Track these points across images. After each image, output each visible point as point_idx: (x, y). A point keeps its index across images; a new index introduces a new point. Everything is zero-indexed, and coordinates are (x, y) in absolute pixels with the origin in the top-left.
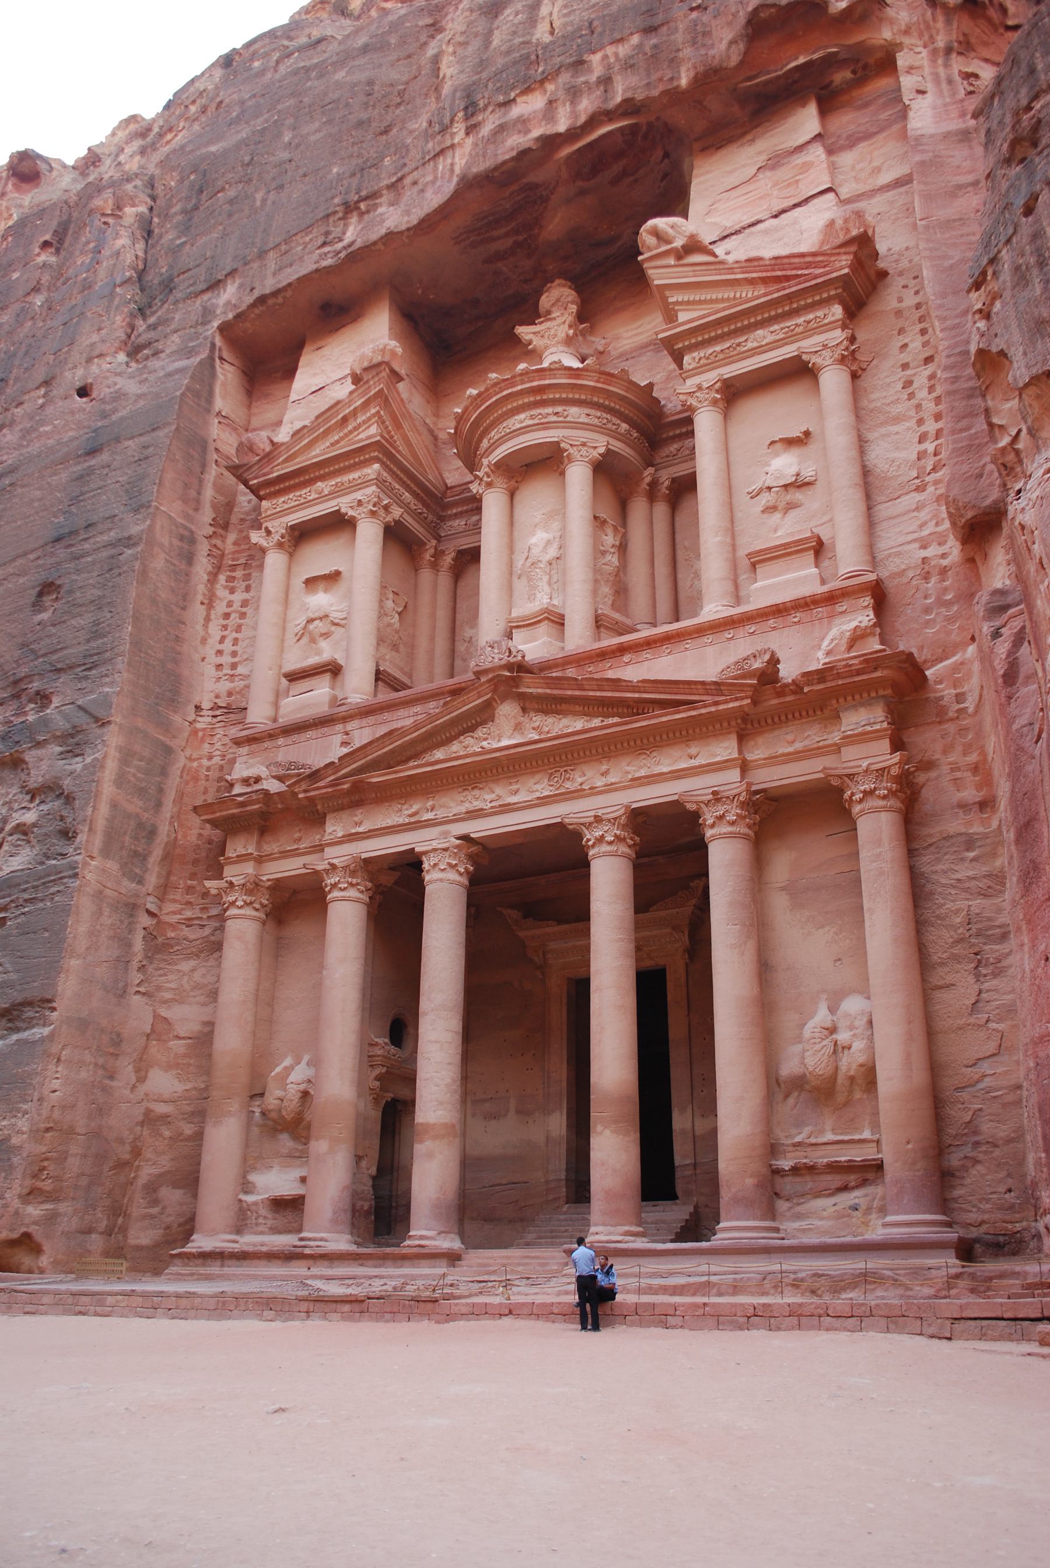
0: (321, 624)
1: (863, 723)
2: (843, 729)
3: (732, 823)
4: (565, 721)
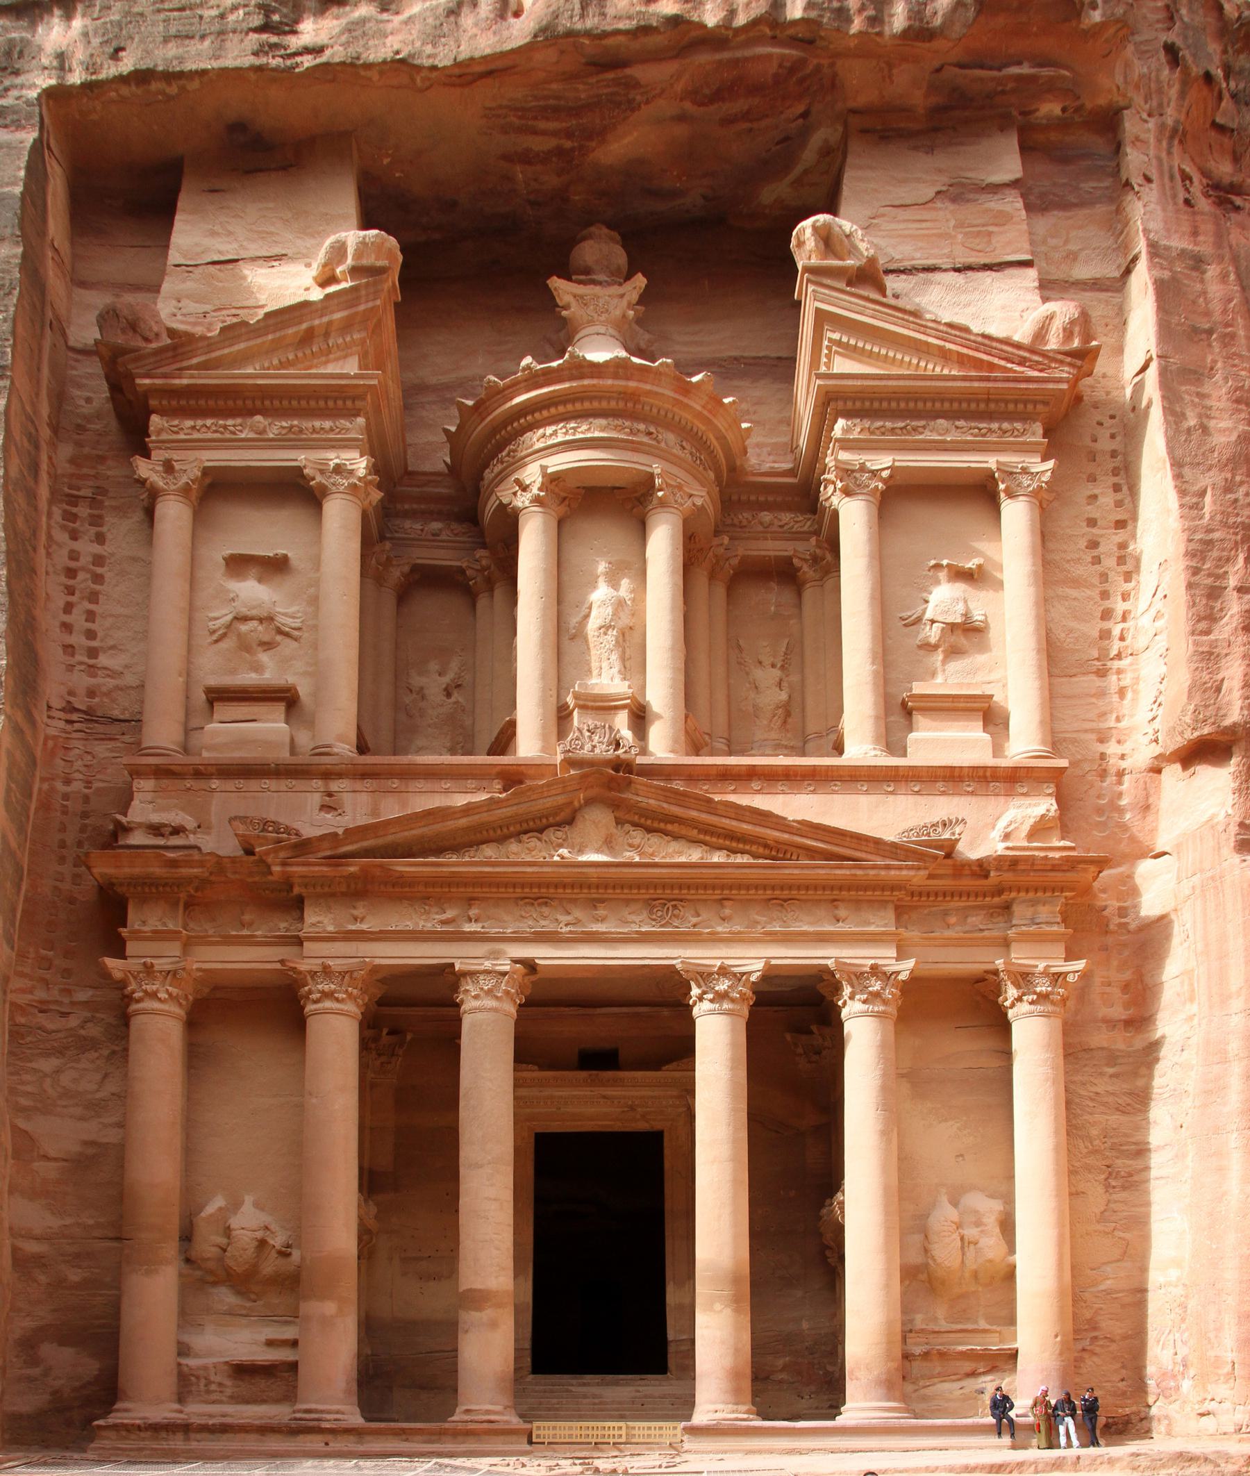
0: (260, 628)
1: (1038, 921)
2: (1014, 922)
3: (885, 1002)
4: (674, 846)
